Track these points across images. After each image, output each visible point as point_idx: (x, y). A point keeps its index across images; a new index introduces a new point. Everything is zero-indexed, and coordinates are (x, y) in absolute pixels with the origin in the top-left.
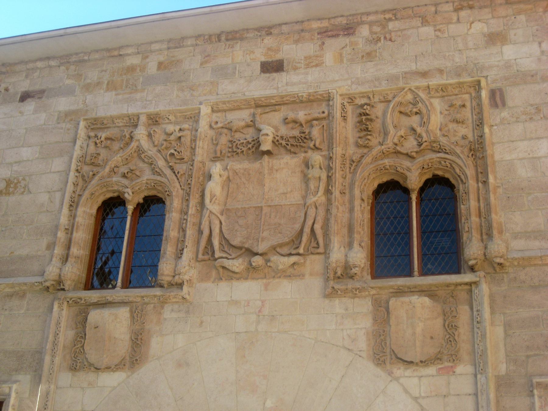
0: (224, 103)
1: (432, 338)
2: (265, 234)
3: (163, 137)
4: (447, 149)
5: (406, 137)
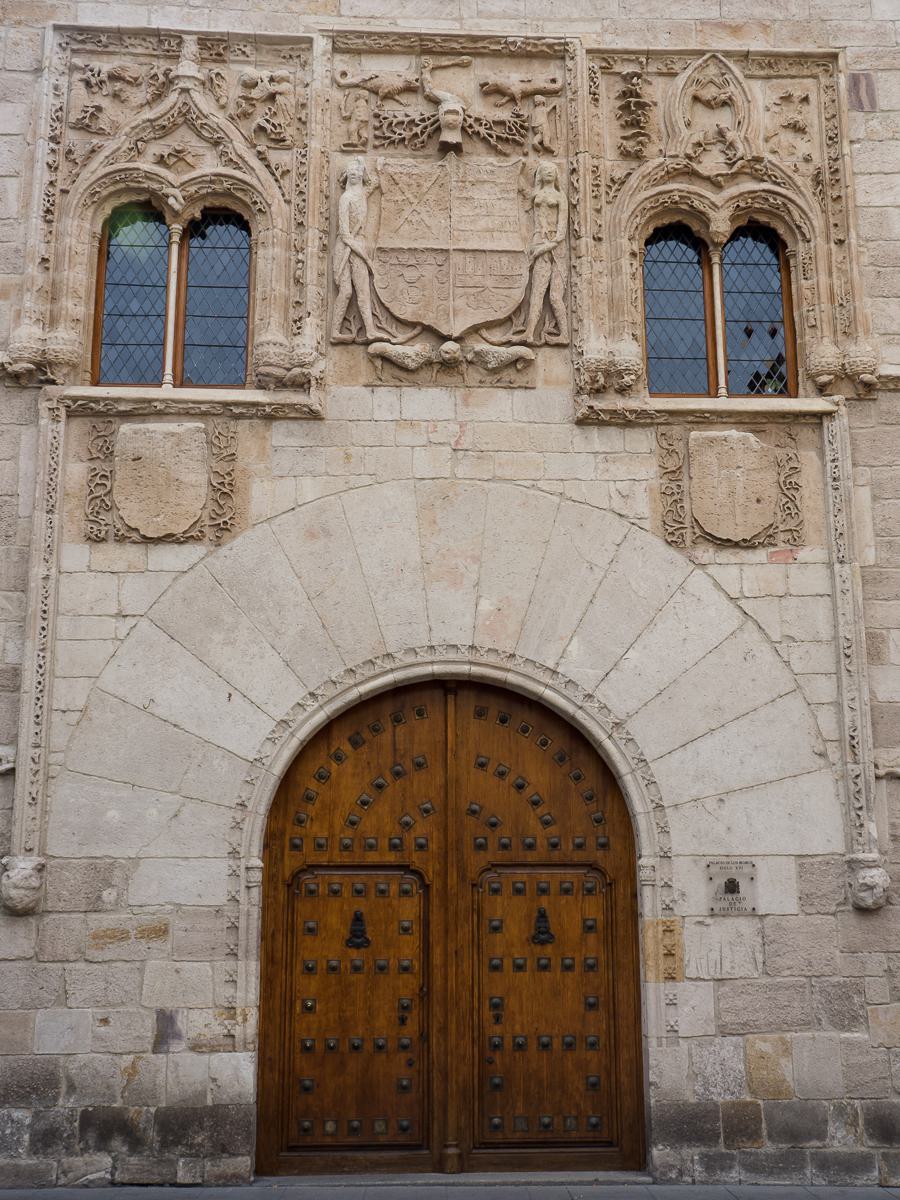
0: (360, 35)
1: (758, 501)
2: (460, 303)
3: (239, 91)
4: (778, 176)
5: (708, 148)
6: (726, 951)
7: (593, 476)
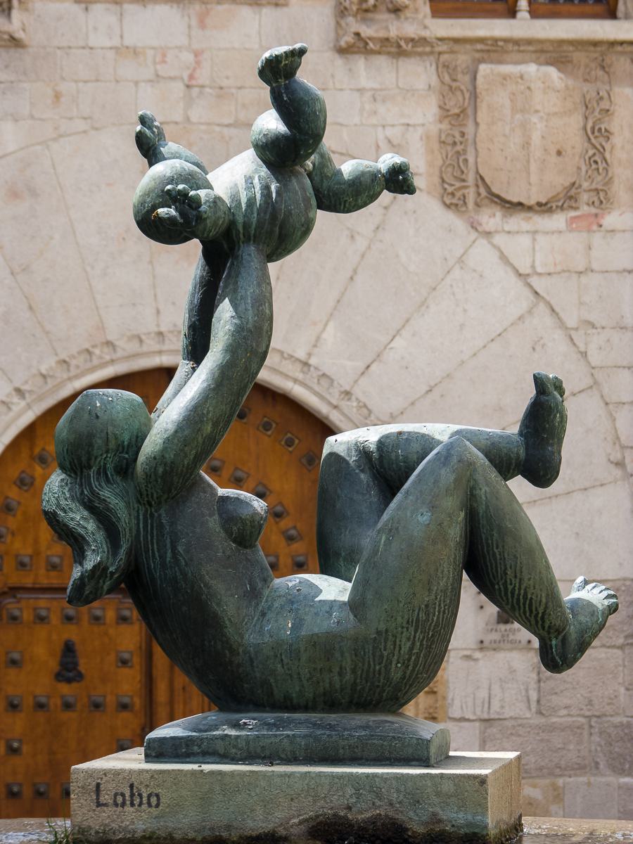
1: (559, 153)
6: (496, 689)
7: (357, 120)
